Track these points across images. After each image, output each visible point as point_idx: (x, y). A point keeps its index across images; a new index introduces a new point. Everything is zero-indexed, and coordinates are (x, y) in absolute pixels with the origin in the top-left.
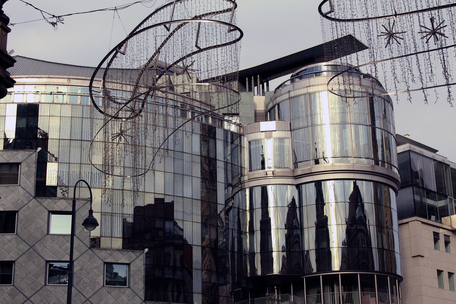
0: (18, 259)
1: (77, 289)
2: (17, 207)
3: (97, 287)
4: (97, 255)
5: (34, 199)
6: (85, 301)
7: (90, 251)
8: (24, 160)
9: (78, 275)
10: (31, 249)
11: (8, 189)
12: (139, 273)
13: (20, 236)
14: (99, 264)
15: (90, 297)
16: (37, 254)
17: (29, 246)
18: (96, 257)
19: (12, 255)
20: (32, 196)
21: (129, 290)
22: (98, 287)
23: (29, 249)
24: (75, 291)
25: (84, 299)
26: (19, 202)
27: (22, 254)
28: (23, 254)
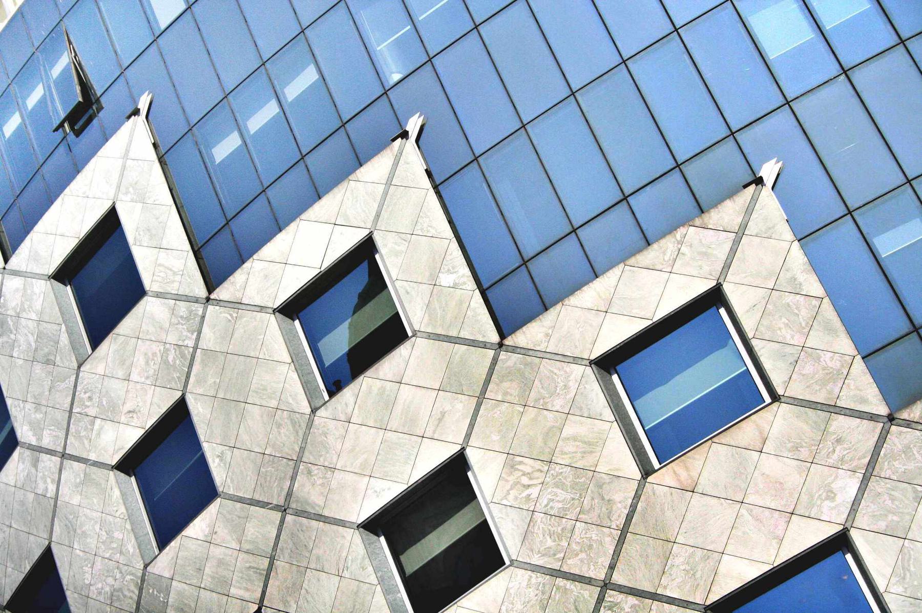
0: (264, 593)
1: (535, 568)
2: (173, 385)
3: (617, 497)
4: (544, 355)
5: (210, 308)
6: (600, 600)
7: (507, 360)
8: (119, 187)
9: (511, 497)
10: (289, 518)
11: (121, 339)
12: (790, 299)
13: (231, 492)
14: (573, 386)
15: (612, 567)
16: (314, 523)
17: (277, 508)
18: (547, 367)
19: (241, 593)
20: (196, 300)
21: (783, 409)
22: (622, 496)
23: (282, 521)
24: (534, 581)
25: (586, 594)
26: (170, 358)
27: (266, 562)
28: (272, 559)
